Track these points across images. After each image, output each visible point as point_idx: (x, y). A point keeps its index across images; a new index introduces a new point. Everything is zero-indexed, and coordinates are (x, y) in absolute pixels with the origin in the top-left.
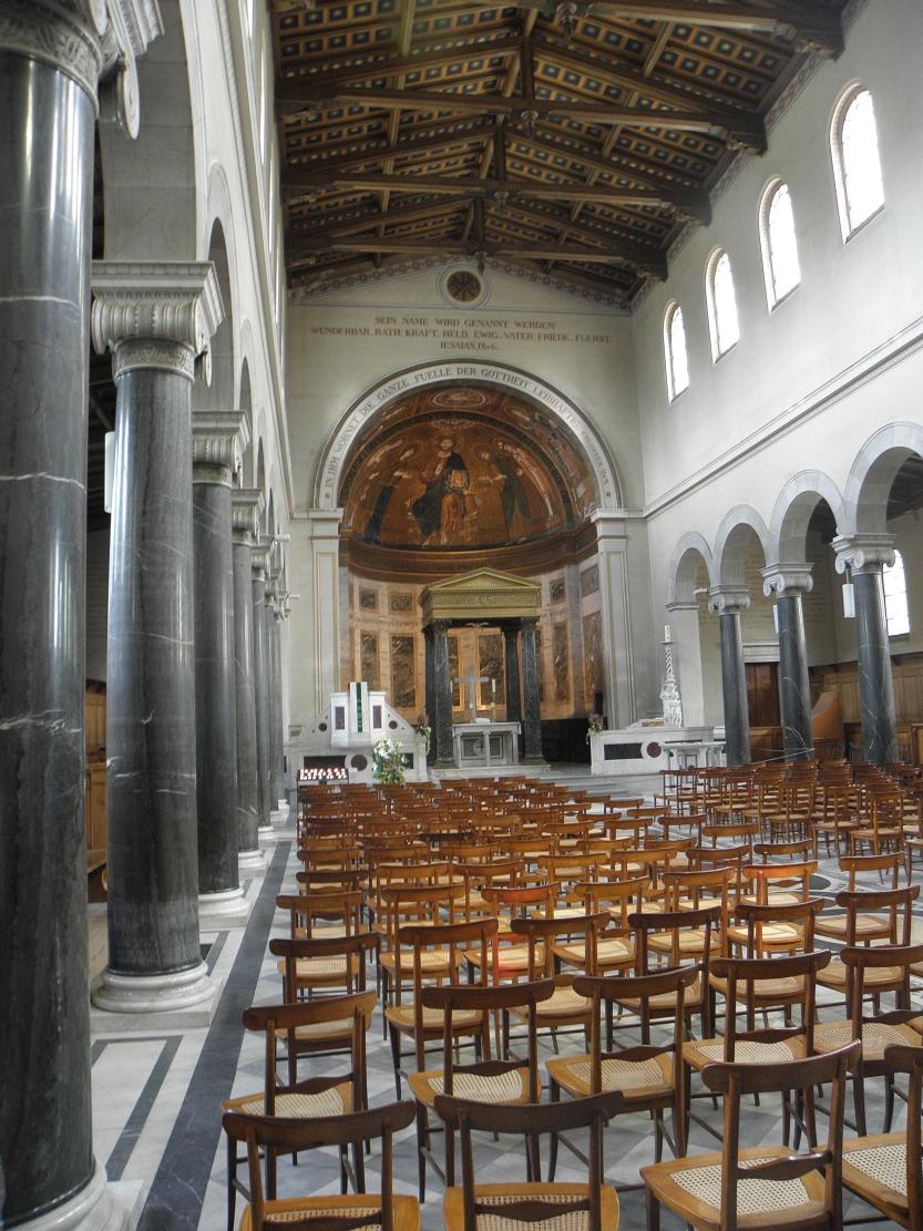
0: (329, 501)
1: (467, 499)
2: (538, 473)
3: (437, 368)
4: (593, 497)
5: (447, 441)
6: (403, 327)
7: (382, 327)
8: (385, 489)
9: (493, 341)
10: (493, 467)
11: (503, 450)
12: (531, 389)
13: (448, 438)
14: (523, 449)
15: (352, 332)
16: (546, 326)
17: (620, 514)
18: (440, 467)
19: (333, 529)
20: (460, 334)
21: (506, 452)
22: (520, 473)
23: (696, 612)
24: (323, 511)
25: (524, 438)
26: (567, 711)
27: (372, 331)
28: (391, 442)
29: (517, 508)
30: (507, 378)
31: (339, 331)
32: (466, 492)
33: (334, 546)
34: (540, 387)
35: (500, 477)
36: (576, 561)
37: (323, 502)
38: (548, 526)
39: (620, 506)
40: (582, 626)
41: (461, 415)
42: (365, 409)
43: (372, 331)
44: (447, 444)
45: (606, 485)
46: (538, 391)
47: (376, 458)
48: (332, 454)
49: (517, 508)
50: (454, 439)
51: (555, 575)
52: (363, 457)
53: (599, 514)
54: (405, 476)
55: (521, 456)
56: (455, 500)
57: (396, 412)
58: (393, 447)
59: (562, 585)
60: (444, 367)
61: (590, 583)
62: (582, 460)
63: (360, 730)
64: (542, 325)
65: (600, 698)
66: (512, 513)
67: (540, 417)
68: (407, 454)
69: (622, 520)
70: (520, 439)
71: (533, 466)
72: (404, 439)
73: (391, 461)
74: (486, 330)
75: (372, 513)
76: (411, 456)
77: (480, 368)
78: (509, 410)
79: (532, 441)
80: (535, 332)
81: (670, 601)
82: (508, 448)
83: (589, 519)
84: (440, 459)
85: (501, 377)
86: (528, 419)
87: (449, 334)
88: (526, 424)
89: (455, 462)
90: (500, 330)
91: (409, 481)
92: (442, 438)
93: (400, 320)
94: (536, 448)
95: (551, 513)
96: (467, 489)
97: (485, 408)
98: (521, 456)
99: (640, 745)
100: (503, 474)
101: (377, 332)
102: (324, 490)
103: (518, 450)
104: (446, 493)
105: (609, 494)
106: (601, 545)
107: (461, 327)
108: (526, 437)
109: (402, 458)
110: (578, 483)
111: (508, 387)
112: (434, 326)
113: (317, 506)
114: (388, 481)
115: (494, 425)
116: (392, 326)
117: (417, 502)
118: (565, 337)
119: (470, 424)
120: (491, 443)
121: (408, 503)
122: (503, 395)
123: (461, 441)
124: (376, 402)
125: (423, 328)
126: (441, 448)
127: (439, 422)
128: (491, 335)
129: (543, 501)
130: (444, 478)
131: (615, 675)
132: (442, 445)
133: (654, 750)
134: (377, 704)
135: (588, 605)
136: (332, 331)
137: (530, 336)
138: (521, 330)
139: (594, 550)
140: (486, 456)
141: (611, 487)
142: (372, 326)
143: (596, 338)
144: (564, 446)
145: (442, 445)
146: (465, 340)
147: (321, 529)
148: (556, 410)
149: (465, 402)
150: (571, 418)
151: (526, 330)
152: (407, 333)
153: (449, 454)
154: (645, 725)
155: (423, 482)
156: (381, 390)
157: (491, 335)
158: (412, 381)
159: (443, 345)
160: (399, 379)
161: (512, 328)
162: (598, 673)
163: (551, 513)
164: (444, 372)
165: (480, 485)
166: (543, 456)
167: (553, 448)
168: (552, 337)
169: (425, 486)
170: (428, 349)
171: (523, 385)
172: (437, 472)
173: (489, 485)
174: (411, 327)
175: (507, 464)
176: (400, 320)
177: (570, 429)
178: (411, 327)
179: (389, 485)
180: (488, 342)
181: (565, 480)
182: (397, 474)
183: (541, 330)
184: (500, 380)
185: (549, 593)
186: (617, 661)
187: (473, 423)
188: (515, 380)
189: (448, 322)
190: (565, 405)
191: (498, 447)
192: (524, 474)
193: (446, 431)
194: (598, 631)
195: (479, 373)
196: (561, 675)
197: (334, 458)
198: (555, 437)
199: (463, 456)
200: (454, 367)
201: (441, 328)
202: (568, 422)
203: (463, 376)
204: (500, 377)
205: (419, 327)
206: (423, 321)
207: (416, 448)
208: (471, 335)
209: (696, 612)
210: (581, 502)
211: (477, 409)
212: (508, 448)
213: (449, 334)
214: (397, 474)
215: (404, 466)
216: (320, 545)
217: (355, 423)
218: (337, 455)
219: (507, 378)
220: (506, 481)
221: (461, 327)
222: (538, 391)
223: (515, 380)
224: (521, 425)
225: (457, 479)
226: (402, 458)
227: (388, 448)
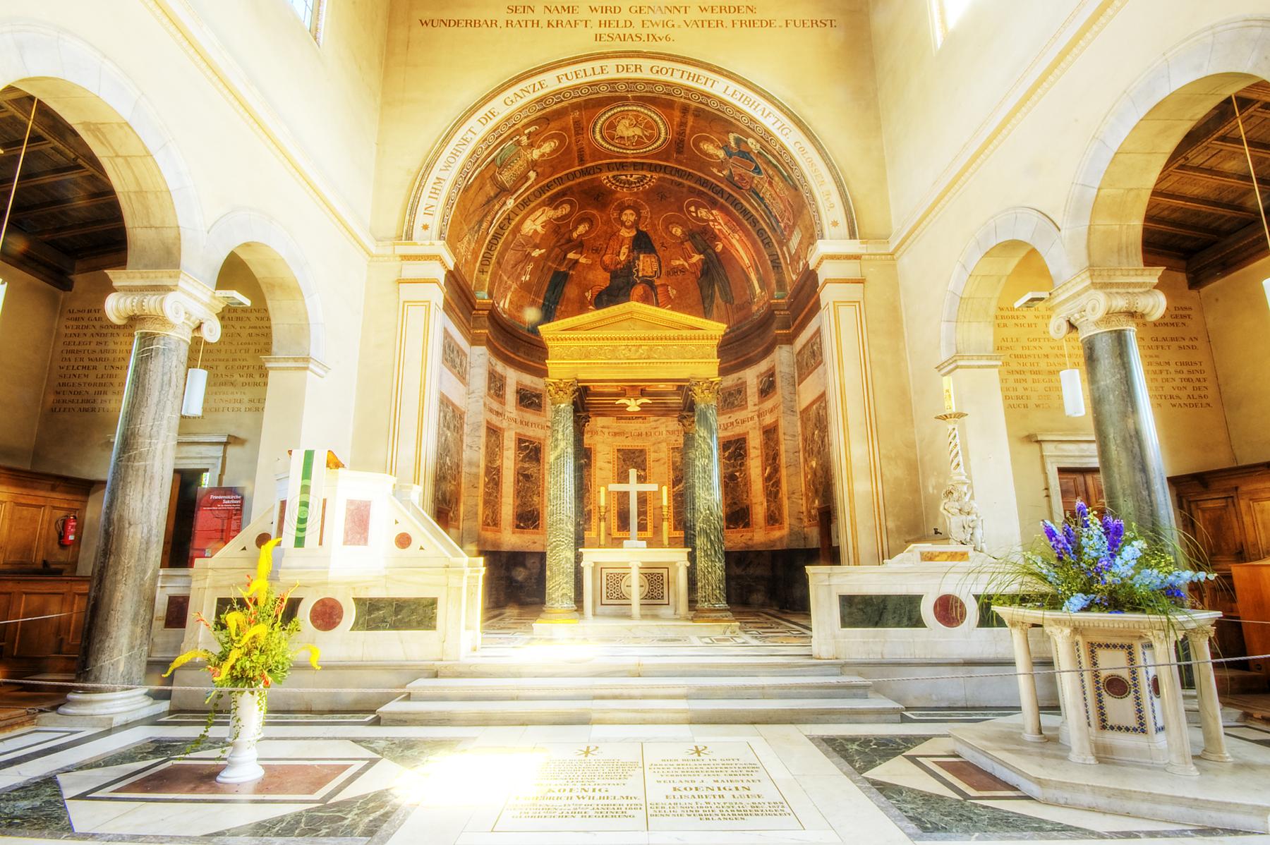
0: (427, 233)
1: (659, 290)
2: (740, 241)
3: (588, 66)
4: (811, 237)
5: (628, 212)
6: (544, 17)
7: (515, 17)
8: (557, 274)
9: (666, 31)
10: (688, 245)
11: (697, 218)
12: (720, 88)
13: (629, 207)
14: (722, 209)
15: (475, 24)
16: (744, 9)
17: (854, 247)
18: (624, 250)
19: (441, 275)
20: (621, 24)
21: (701, 220)
22: (719, 247)
23: (996, 371)
24: (415, 244)
25: (721, 192)
26: (779, 536)
27: (501, 23)
28: (553, 202)
29: (717, 294)
30: (686, 75)
31: (457, 23)
32: (657, 282)
33: (437, 295)
34: (733, 86)
35: (696, 258)
36: (790, 340)
37: (418, 231)
38: (755, 308)
39: (852, 235)
40: (799, 424)
41: (636, 166)
42: (487, 118)
43: (501, 23)
44: (629, 216)
45: (829, 208)
46: (730, 91)
47: (535, 224)
48: (435, 173)
49: (717, 294)
50: (636, 209)
51: (763, 366)
52: (512, 215)
53: (822, 247)
54: (583, 260)
55: (718, 221)
56: (645, 292)
57: (548, 147)
58: (560, 213)
59: (773, 375)
60: (597, 64)
61: (811, 360)
62: (796, 189)
63: (321, 544)
64: (738, 9)
65: (827, 517)
66: (712, 302)
67: (738, 141)
68: (582, 229)
69: (857, 257)
70: (712, 195)
71: (734, 231)
72: (571, 203)
73: (557, 229)
74: (658, 17)
75: (541, 301)
76: (586, 232)
77: (646, 63)
78: (696, 145)
79: (730, 195)
80: (727, 18)
81: (944, 358)
82: (703, 213)
83: (807, 265)
84: (624, 238)
85: (677, 74)
86: (721, 154)
87: (608, 24)
88: (721, 165)
89: (642, 243)
90: (678, 18)
91: (589, 267)
92: (622, 208)
93: (539, 9)
94: (736, 203)
95: (758, 290)
96: (659, 277)
97: (664, 154)
98: (718, 221)
99: (920, 597)
100: (700, 254)
101: (508, 23)
102: (420, 219)
103: (714, 212)
104: (634, 283)
105: (835, 224)
106: (828, 295)
107: (624, 16)
108: (722, 189)
109: (575, 235)
110: (791, 232)
111: (688, 90)
112: (583, 14)
113: (409, 237)
114: (560, 264)
115: (681, 177)
116: (530, 16)
117: (600, 294)
118: (769, 24)
119: (653, 178)
120: (681, 210)
121: (589, 295)
122: (685, 109)
123: (646, 212)
124: (502, 108)
125: (572, 17)
126: (623, 224)
127: (610, 175)
128: (665, 24)
129: (748, 279)
130: (630, 266)
131: (850, 478)
132: (624, 218)
133: (948, 610)
134: (359, 496)
135: (807, 393)
136: (448, 24)
137: (719, 23)
138: (707, 16)
139: (816, 308)
140: (678, 231)
141: (839, 214)
142: (502, 16)
143: (814, 23)
144: (770, 184)
145: (624, 218)
146: (628, 31)
147: (413, 270)
148: (757, 115)
149: (640, 142)
150: (779, 124)
151: (716, 16)
152: (549, 24)
153: (634, 233)
154: (928, 557)
155: (606, 269)
156: (509, 93)
157: (665, 24)
158: (551, 82)
159: (598, 37)
160: (535, 80)
161: (694, 14)
162: (823, 486)
163: (758, 290)
164: (598, 70)
165: (674, 271)
166: (745, 212)
167: (757, 195)
168: (752, 24)
169: (609, 274)
170: (580, 41)
171: (710, 83)
172: (622, 258)
173: (682, 270)
174: (554, 17)
175: (702, 238)
176: (539, 9)
177: (777, 140)
178: (554, 17)
179: (562, 269)
180: (660, 32)
181: (774, 241)
182: (571, 255)
183: (736, 16)
184: (676, 79)
185: (755, 390)
186: (853, 460)
187: (656, 176)
188: (696, 78)
189: (605, 10)
190: (770, 108)
191: (690, 212)
192: (724, 246)
193: (624, 194)
194: (821, 424)
195: (646, 71)
196: (773, 492)
197: (437, 178)
198: (759, 173)
199: (651, 234)
200: (611, 64)
201: (599, 16)
202: (774, 129)
203: (624, 75)
204: (678, 76)
205: (565, 17)
206: (570, 10)
207: (590, 220)
208: (637, 23)
209: (996, 371)
210: (795, 258)
211: (655, 156)
212: (703, 213)
213: (608, 24)
214: (571, 255)
215: (580, 246)
216: (408, 291)
217: (470, 135)
218: (443, 175)
219: (686, 75)
220: (704, 262)
221: (621, 17)
222: (730, 91)
223: (696, 78)
224: (715, 170)
225: (646, 265)
226: (575, 235)
227: (550, 213)
